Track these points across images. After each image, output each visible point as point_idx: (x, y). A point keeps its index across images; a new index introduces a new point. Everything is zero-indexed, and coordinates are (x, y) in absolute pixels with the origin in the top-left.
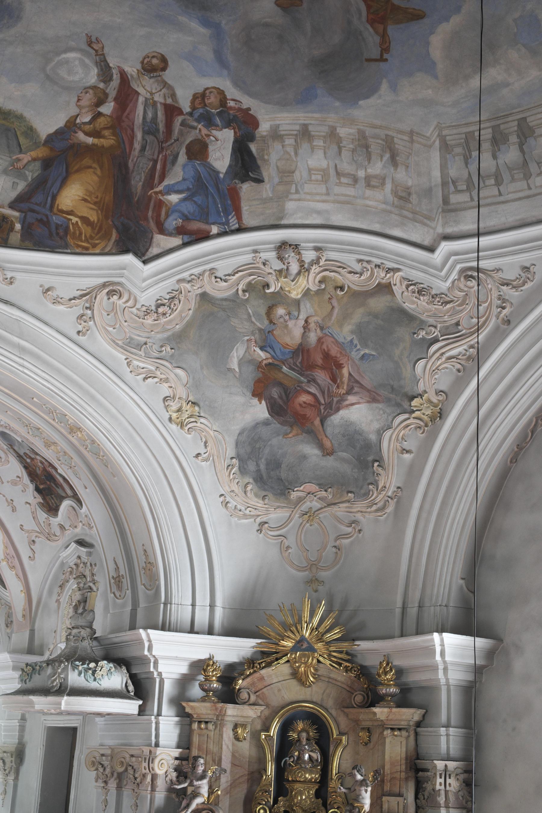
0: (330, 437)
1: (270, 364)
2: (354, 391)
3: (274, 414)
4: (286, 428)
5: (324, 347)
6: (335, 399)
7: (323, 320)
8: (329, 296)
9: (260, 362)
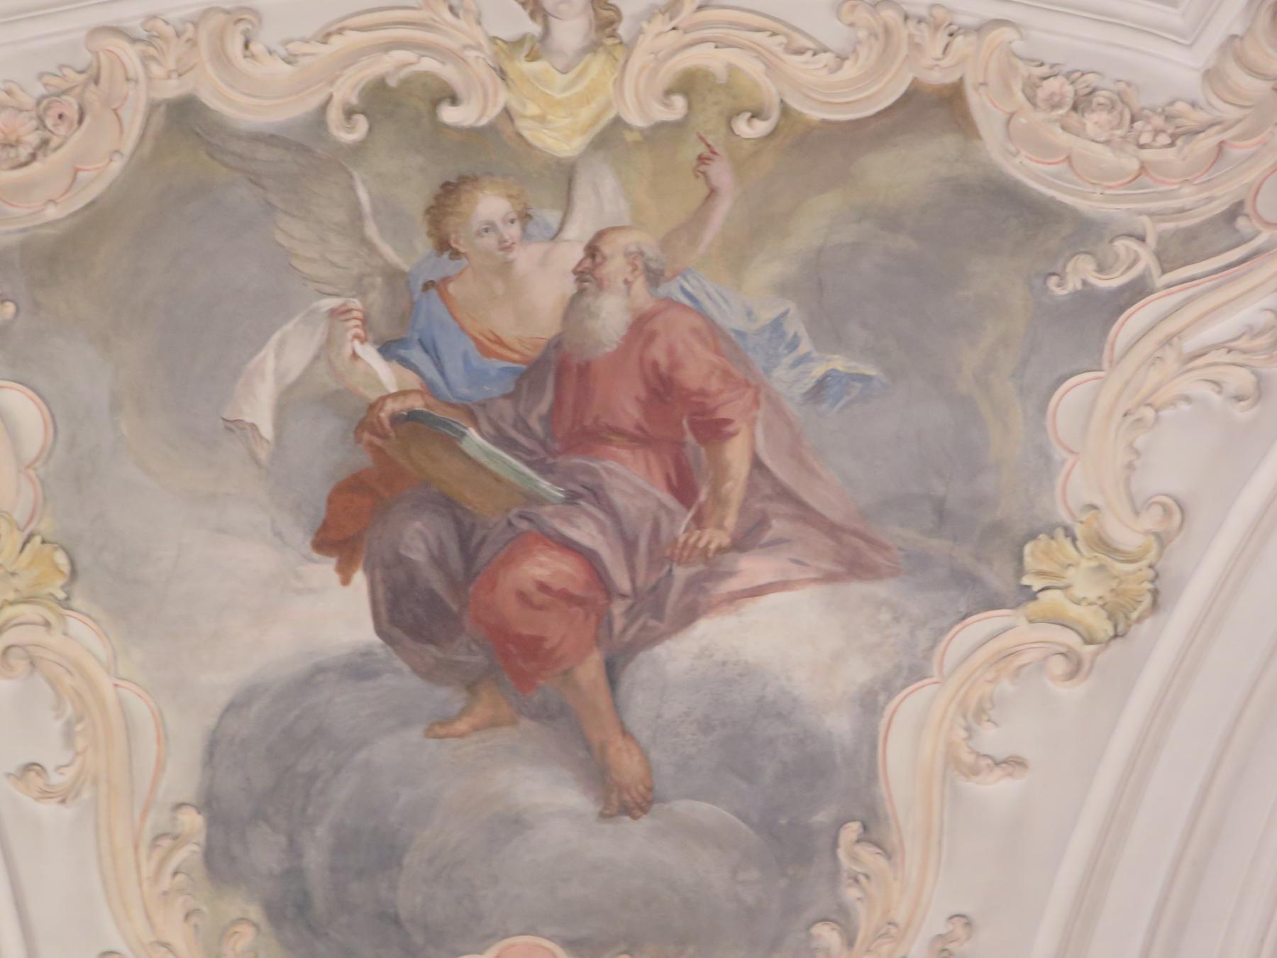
0: (643, 735)
1: (413, 416)
2: (769, 535)
3: (397, 633)
4: (448, 697)
5: (658, 353)
7: (666, 243)
8: (702, 149)
9: (372, 407)
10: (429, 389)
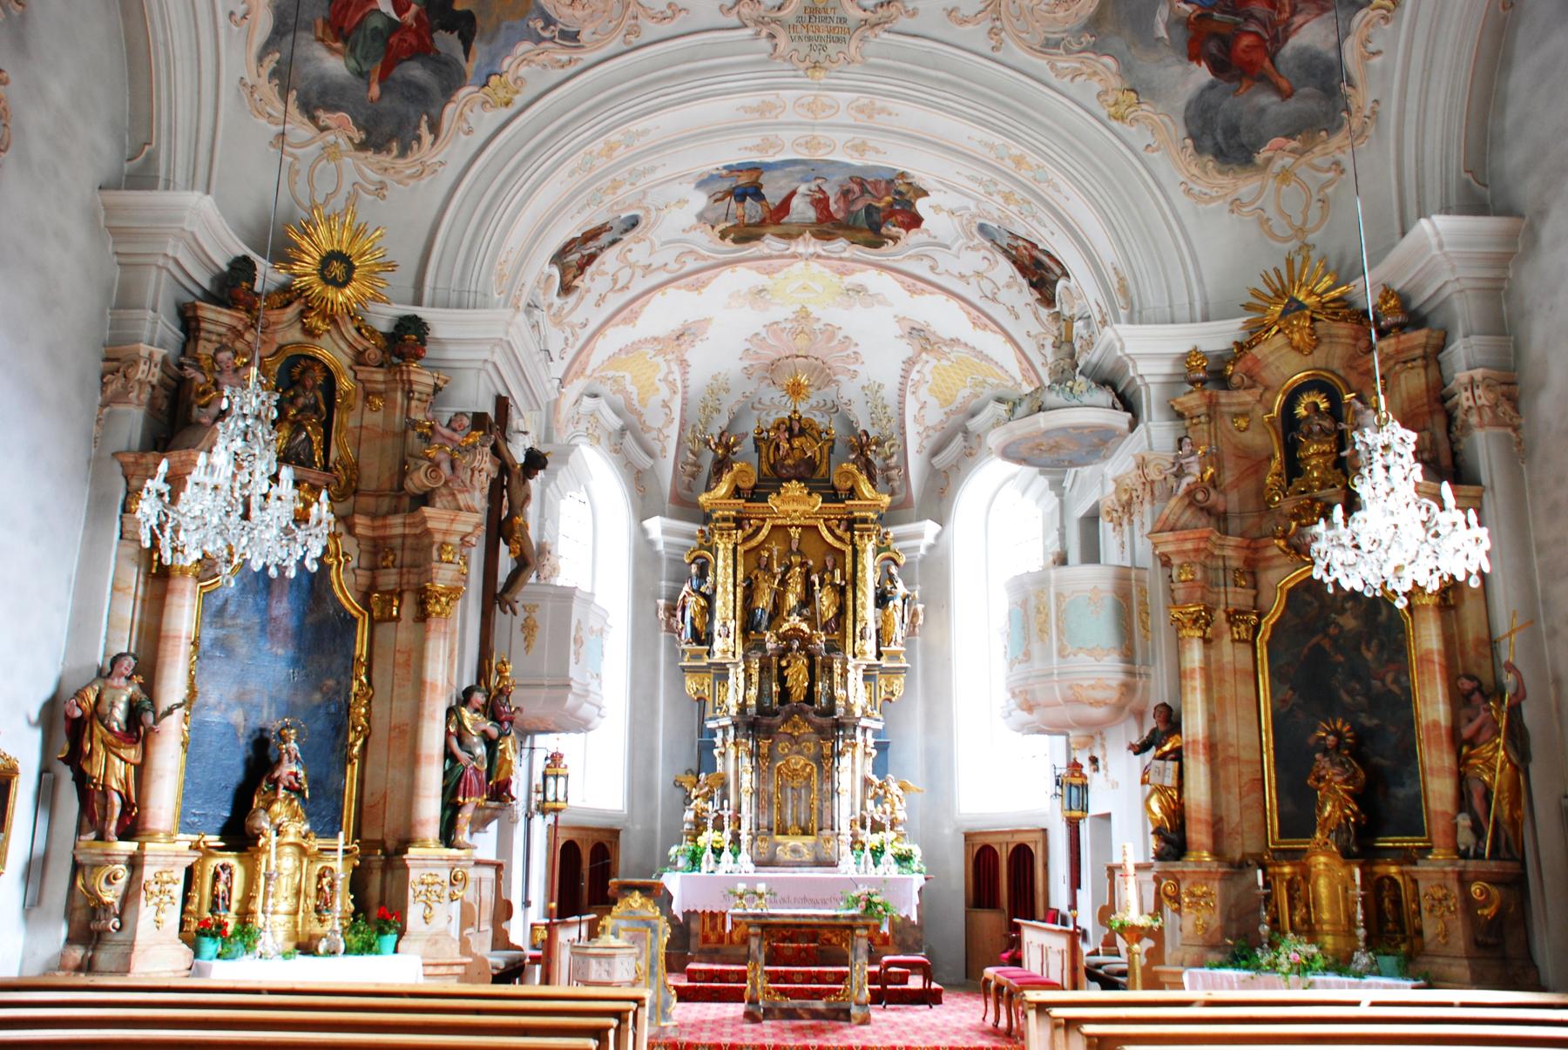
1: (1199, 16)
4: (1236, 84)
6: (1280, 28)
9: (1189, 18)
10: (1200, 7)
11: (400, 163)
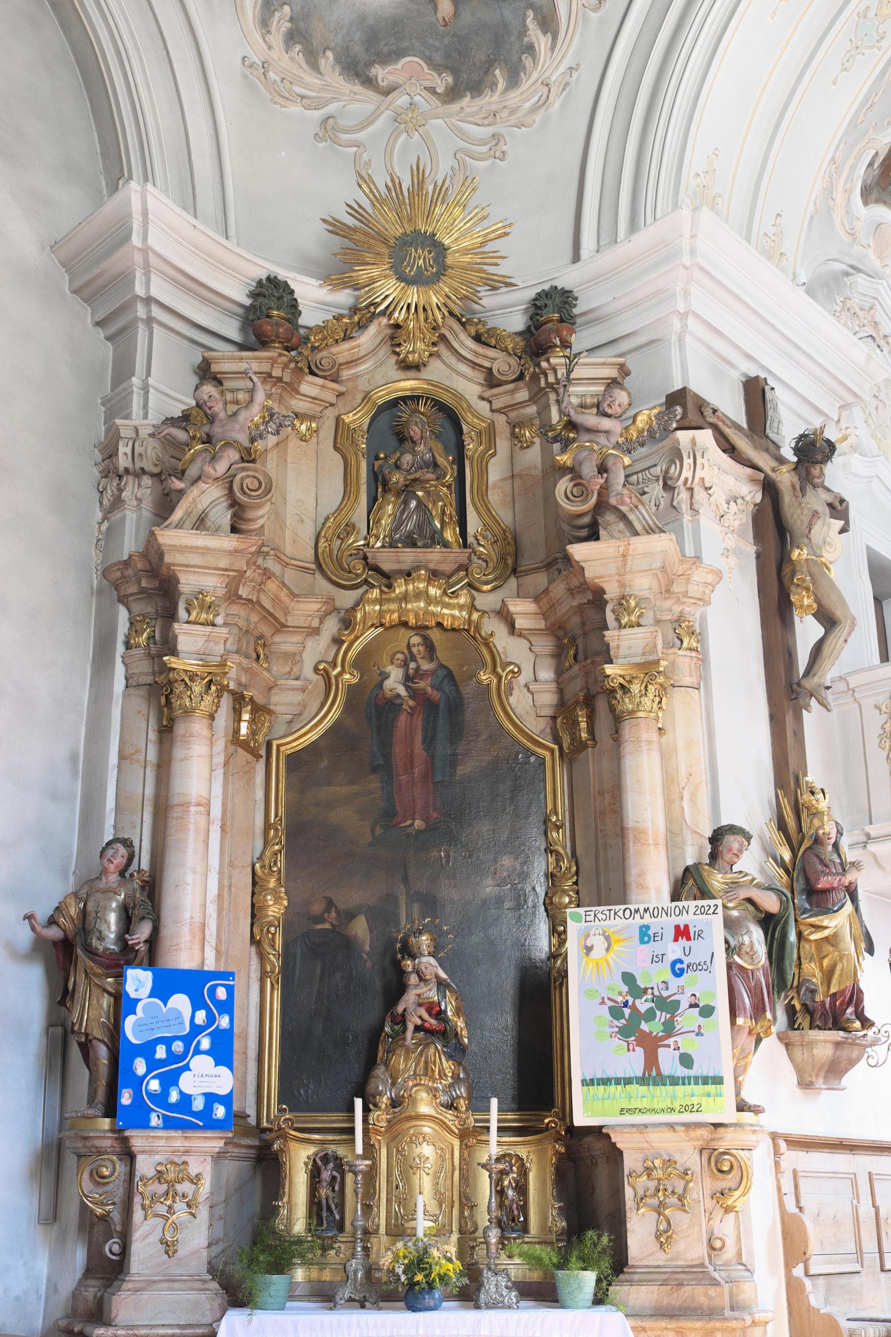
11: (514, 97)
